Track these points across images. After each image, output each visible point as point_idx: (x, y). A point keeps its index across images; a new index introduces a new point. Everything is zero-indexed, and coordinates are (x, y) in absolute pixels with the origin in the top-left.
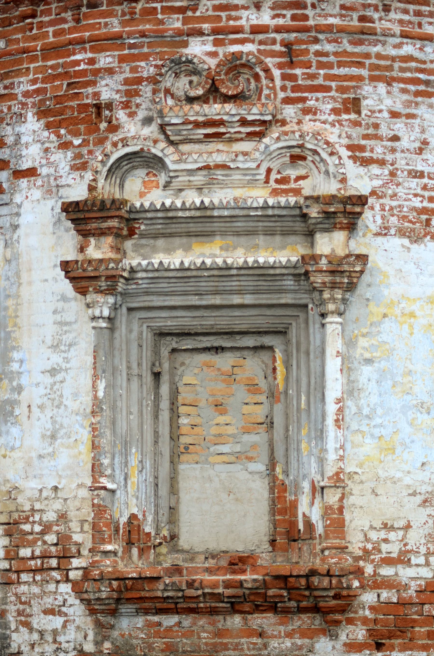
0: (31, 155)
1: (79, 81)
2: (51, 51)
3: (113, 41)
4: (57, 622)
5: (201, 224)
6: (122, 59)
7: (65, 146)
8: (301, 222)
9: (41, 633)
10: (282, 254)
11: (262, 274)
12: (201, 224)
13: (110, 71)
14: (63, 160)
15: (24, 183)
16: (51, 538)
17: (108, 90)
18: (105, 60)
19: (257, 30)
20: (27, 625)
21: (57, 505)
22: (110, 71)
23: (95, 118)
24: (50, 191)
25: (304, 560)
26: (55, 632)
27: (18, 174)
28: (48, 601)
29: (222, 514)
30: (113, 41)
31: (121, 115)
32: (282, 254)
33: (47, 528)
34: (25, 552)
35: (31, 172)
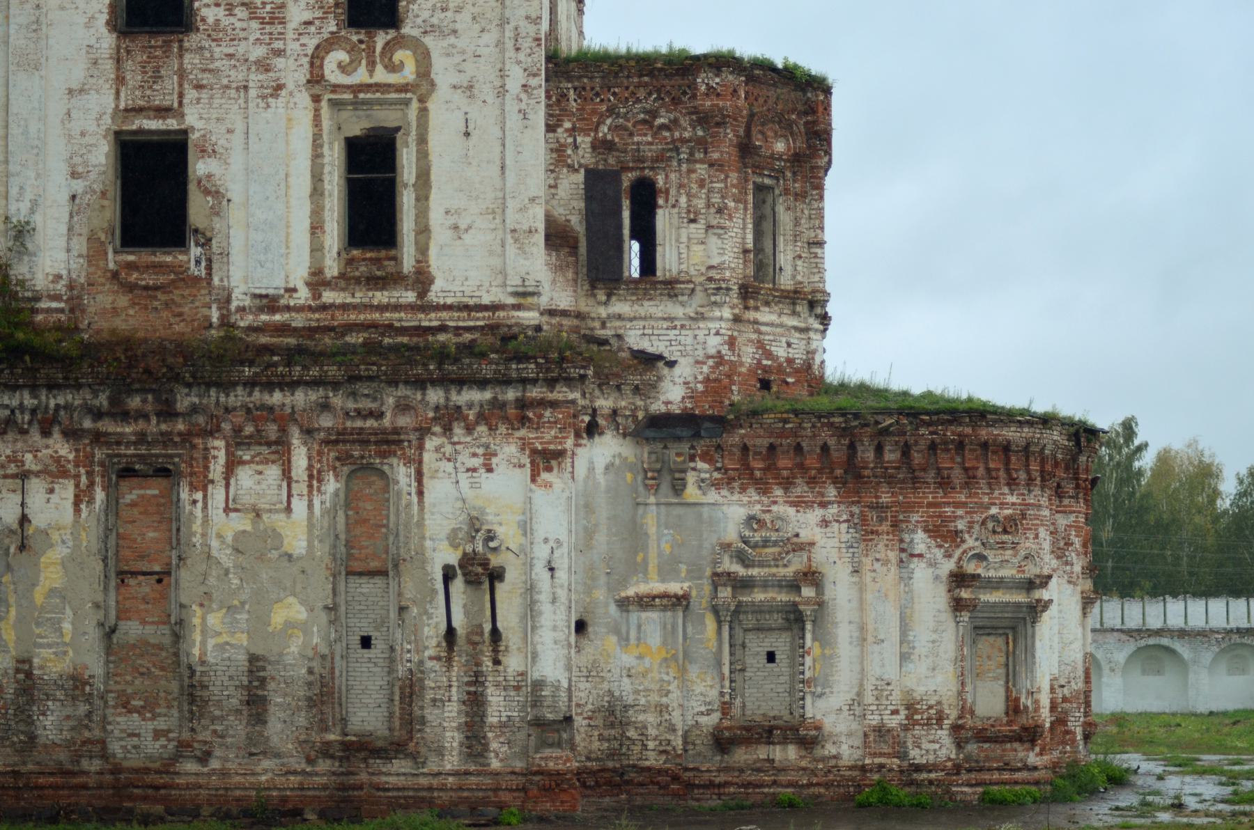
0: (920, 548)
1: (946, 520)
2: (930, 505)
3: (963, 505)
4: (937, 746)
5: (998, 584)
6: (967, 513)
7: (940, 546)
8: (1030, 585)
9: (927, 751)
10: (1020, 598)
11: (1018, 605)
12: (998, 584)
13: (962, 517)
14: (939, 553)
15: (916, 560)
16: (933, 711)
17: (961, 525)
18: (960, 512)
19: (1013, 504)
20: (919, 747)
21: (936, 698)
22: (962, 517)
23: (955, 537)
24: (933, 564)
25: (1023, 720)
26: (935, 751)
27: (912, 555)
28: (931, 738)
29: (989, 702)
30: (963, 505)
31: (967, 536)
32: (1020, 598)
33: (931, 707)
34: (917, 717)
35: (920, 556)
